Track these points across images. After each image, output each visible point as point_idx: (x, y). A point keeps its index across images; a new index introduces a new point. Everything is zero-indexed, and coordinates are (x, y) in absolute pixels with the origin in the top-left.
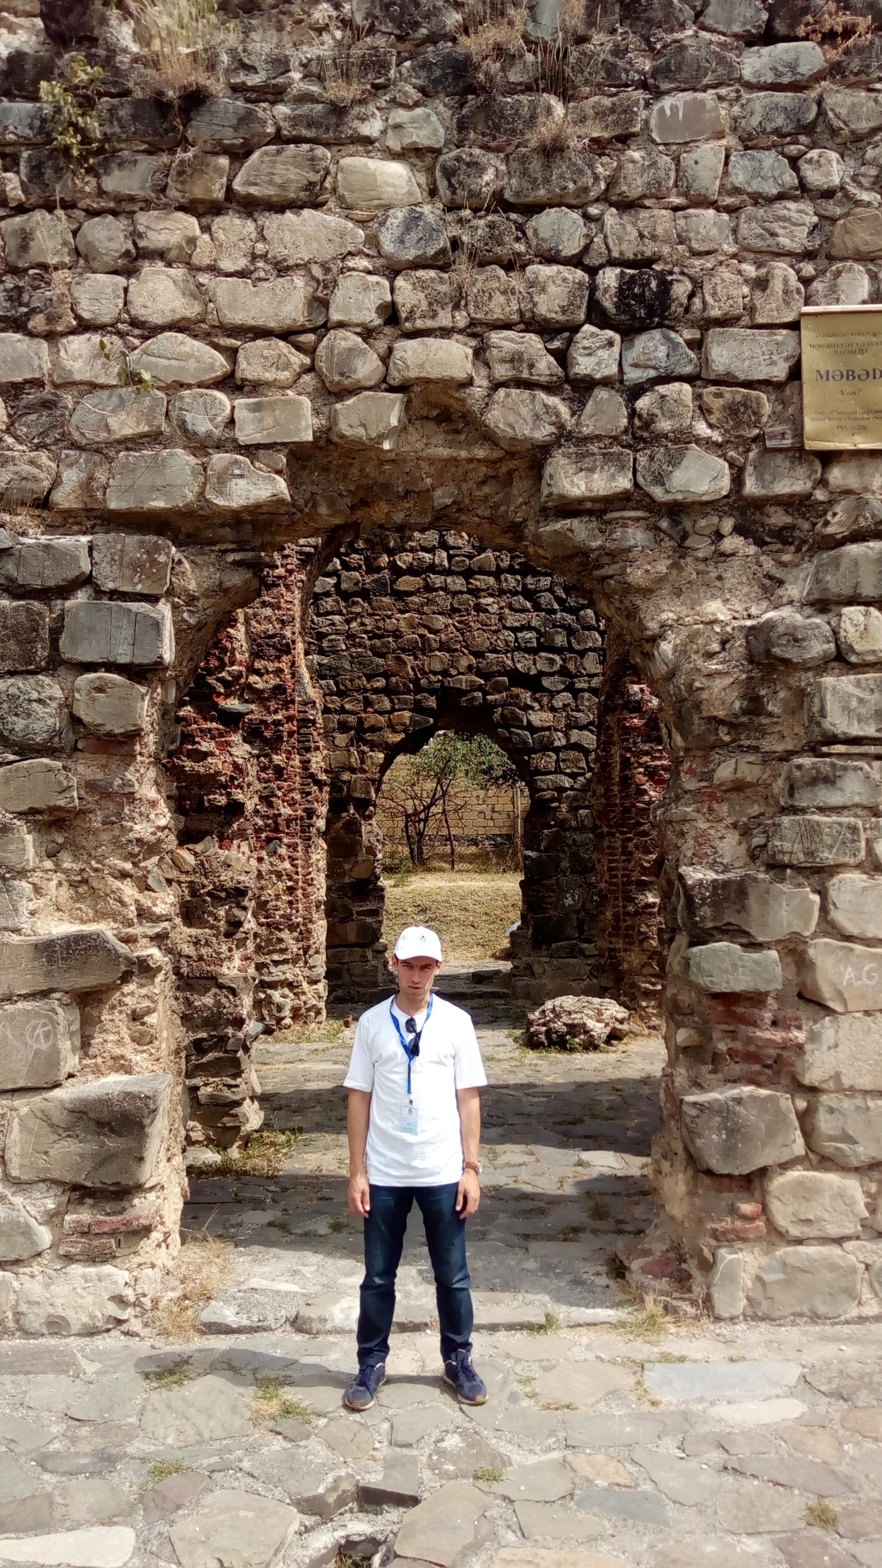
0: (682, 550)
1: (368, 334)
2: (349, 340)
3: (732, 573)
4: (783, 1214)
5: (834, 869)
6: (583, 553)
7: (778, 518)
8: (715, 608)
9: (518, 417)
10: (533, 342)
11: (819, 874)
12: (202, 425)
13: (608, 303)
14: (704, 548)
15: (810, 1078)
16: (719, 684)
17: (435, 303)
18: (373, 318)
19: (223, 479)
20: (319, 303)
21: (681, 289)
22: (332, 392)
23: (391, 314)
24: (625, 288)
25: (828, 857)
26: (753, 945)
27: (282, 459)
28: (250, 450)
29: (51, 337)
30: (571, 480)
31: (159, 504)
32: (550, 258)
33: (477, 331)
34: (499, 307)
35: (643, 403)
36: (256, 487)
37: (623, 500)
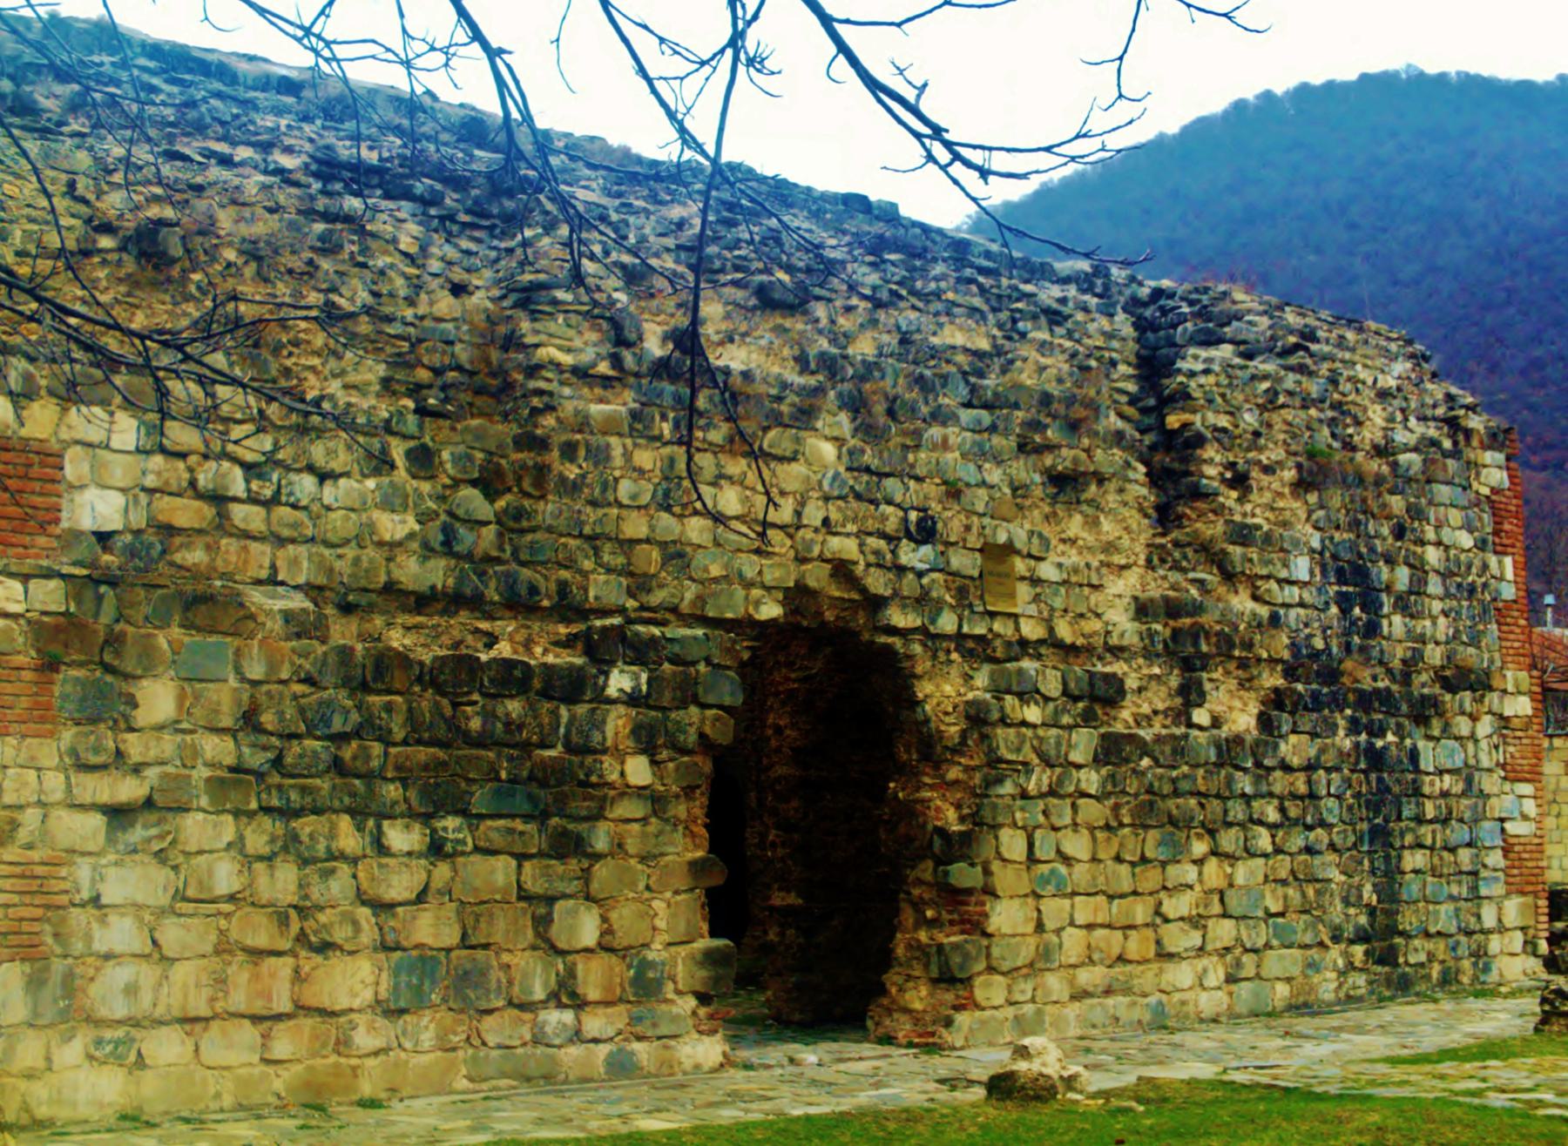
0: (934, 657)
1: (816, 530)
2: (809, 535)
3: (954, 672)
4: (979, 994)
5: (1001, 826)
6: (896, 653)
7: (971, 644)
8: (948, 689)
9: (877, 583)
10: (882, 544)
11: (995, 827)
12: (750, 573)
13: (913, 528)
14: (942, 656)
15: (990, 930)
16: (953, 729)
17: (846, 519)
18: (818, 523)
19: (758, 603)
20: (798, 514)
21: (940, 526)
22: (801, 560)
23: (826, 521)
24: (920, 521)
25: (1000, 820)
26: (972, 865)
27: (780, 596)
28: (768, 589)
29: (681, 516)
30: (899, 618)
31: (729, 615)
32: (890, 502)
33: (862, 534)
34: (871, 525)
35: (925, 581)
36: (770, 610)
37: (914, 630)
